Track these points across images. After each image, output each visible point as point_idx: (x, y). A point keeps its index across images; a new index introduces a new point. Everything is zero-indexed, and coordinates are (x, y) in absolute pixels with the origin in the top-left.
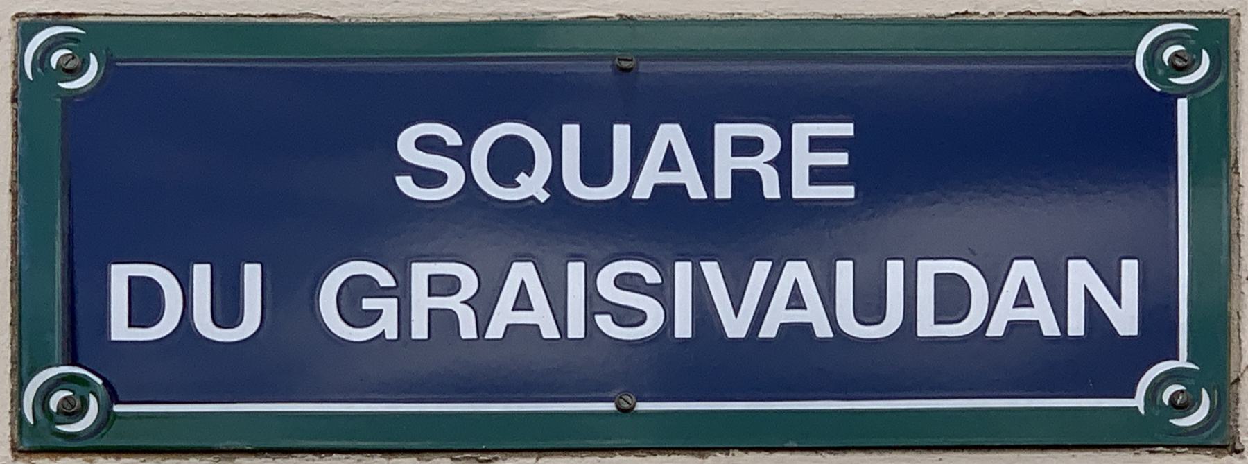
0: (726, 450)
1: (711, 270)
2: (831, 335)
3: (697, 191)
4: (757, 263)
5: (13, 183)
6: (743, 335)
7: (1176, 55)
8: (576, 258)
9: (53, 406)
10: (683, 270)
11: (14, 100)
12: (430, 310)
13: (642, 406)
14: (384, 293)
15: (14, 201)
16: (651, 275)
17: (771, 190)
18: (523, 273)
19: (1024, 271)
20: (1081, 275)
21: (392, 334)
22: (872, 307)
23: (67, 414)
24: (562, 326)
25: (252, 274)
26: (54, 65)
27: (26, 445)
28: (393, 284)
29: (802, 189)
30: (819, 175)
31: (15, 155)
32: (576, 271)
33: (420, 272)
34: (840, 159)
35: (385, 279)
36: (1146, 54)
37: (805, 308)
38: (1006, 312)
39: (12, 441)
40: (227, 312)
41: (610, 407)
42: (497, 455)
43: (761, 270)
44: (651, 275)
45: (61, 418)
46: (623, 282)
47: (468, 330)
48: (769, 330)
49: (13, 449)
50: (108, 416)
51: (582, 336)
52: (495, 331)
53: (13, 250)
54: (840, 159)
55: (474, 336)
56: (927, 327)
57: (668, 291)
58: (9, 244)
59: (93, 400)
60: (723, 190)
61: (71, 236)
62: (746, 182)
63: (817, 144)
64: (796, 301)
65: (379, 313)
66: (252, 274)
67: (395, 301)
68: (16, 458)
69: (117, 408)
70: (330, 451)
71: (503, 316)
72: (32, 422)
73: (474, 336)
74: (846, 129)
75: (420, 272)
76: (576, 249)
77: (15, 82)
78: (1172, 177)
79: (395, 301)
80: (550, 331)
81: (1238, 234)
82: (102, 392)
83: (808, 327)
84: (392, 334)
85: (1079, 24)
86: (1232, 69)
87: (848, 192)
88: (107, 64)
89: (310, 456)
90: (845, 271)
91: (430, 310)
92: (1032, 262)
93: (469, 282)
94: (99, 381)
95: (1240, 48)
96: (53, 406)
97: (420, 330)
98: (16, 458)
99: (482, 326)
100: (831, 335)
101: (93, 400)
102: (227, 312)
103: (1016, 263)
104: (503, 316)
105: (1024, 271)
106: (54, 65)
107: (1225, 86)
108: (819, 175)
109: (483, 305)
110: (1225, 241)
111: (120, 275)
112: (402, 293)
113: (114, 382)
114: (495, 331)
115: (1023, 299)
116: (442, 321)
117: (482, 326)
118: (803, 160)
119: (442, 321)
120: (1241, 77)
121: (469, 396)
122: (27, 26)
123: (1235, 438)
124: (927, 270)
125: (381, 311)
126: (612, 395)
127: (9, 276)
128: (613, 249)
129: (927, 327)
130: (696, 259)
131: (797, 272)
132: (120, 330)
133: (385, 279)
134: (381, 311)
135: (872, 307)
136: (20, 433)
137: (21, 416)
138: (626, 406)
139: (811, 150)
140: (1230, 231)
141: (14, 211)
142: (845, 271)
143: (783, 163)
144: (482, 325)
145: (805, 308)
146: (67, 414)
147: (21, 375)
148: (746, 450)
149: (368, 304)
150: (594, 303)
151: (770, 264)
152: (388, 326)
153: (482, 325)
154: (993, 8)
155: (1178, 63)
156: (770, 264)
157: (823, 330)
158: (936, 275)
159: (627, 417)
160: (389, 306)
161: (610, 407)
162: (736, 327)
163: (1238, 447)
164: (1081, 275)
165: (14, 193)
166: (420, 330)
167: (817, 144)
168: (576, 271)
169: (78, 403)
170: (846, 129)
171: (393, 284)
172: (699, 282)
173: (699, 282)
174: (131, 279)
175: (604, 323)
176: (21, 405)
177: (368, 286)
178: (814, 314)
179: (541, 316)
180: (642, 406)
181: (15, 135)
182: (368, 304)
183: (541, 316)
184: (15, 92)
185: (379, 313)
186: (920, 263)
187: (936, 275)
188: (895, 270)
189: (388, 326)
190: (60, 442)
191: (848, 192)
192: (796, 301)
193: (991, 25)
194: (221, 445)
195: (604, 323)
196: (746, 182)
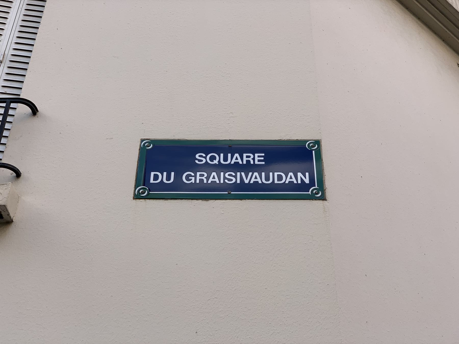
0: (245, 199)
1: (243, 174)
2: (261, 183)
3: (241, 163)
4: (250, 173)
5: (138, 161)
6: (248, 183)
7: (312, 145)
8: (222, 172)
9: (140, 192)
10: (238, 174)
11: (139, 150)
12: (199, 179)
13: (232, 193)
14: (193, 176)
15: (138, 164)
16: (234, 174)
17: (252, 162)
18: (214, 174)
19: (291, 174)
20: (300, 175)
21: (193, 182)
22: (267, 179)
23: (142, 193)
24: (220, 181)
25: (173, 174)
26: (146, 145)
27: (135, 198)
28: (194, 175)
29: (257, 162)
30: (259, 161)
31: (138, 157)
32: (222, 174)
33: (198, 174)
34: (263, 158)
35: (193, 174)
36: (308, 145)
37: (257, 179)
38: (288, 180)
39: (133, 197)
40: (168, 178)
41: (227, 193)
42: (209, 200)
43: (250, 174)
44: (234, 174)
45: (141, 194)
46: (229, 175)
47: (205, 181)
48: (252, 182)
49: (133, 198)
50: (148, 194)
51: (223, 183)
52: (209, 182)
53: (137, 170)
54: (263, 158)
55: (206, 182)
56: (276, 182)
57: (236, 176)
58: (136, 169)
59: (146, 191)
60: (245, 162)
61: (146, 168)
62: (248, 162)
63: (259, 156)
64: (256, 178)
65: (191, 179)
66: (173, 174)
67: (194, 177)
68: (133, 199)
69: (150, 192)
70: (183, 199)
71: (211, 180)
72: (137, 194)
73: (206, 182)
74: (263, 155)
75: (198, 174)
76: (223, 171)
77: (140, 147)
78: (313, 161)
79: (194, 177)
80: (218, 182)
81: (323, 169)
82: (148, 190)
83: (258, 182)
84: (193, 182)
85: (297, 141)
86: (321, 147)
87: (264, 163)
88: (154, 145)
89: (180, 200)
90: (263, 174)
91: (199, 179)
92: (292, 173)
93: (206, 175)
94: (148, 188)
95: (322, 144)
96: (140, 192)
97: (198, 182)
98: (133, 199)
99: (207, 181)
100: (261, 183)
101: (146, 191)
102: (168, 178)
103: (289, 173)
104: (211, 180)
105: (291, 174)
106: (146, 145)
107: (320, 149)
108: (259, 161)
109: (208, 178)
110: (322, 170)
111: (152, 174)
112: (195, 177)
113: (149, 188)
114: (209, 182)
115: (291, 178)
116: (201, 180)
117: (207, 181)
118: (257, 159)
119: (201, 180)
120: (322, 148)
121: (204, 191)
122: (142, 140)
123: (326, 198)
124: (276, 174)
125: (192, 179)
126: (227, 191)
127: (136, 174)
128: (228, 171)
129: (276, 182)
130: (241, 172)
131: (256, 174)
132: (152, 181)
133: (193, 174)
134: (192, 179)
135: (267, 179)
136: (135, 195)
137: (135, 193)
138: (229, 193)
139: (258, 157)
140: (322, 169)
141: (138, 165)
142: (263, 174)
143: (254, 159)
144: (207, 181)
145: (257, 179)
146: (142, 193)
147: (135, 188)
148: (248, 199)
149: (190, 178)
150: (225, 178)
151: (252, 173)
152: (193, 181)
153: (207, 181)
154: (285, 139)
155: (312, 146)
156: (252, 173)
157: (260, 182)
158: (277, 174)
159: (230, 195)
160: (193, 178)
161: (227, 193)
162: (247, 181)
163: (326, 199)
164: (300, 175)
165: (138, 162)
166: (198, 182)
167: (259, 156)
168: (222, 174)
169: (144, 192)
170: (263, 155)
171: (194, 175)
172: (241, 175)
173: (241, 175)
174: (154, 174)
175: (226, 181)
176: (135, 192)
177: (190, 175)
178: (259, 180)
179: (217, 180)
180: (232, 193)
181: (139, 155)
182: (190, 178)
183: (217, 180)
184: (140, 149)
185: (191, 179)
186: (275, 173)
187: (277, 174)
188: (271, 174)
189: (193, 181)
190: (141, 197)
191: (264, 163)
192: (256, 178)
193: (284, 141)
194: (166, 198)
195: (226, 181)
196: (248, 162)
